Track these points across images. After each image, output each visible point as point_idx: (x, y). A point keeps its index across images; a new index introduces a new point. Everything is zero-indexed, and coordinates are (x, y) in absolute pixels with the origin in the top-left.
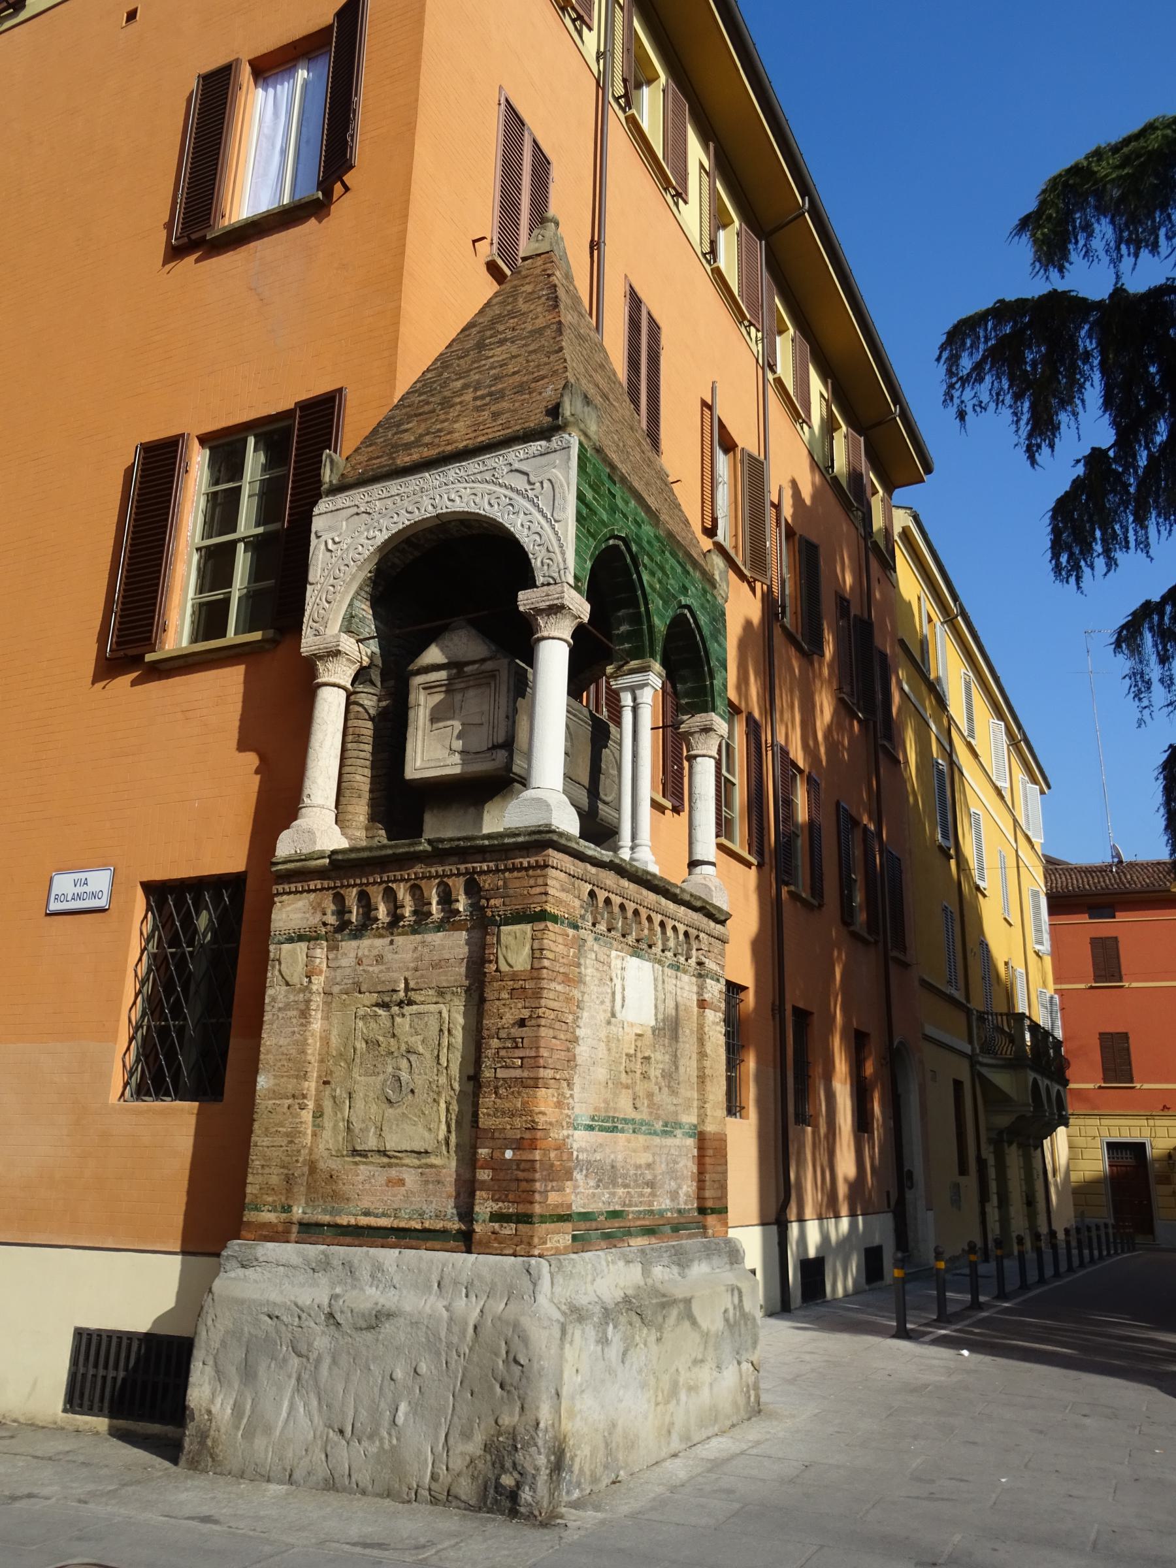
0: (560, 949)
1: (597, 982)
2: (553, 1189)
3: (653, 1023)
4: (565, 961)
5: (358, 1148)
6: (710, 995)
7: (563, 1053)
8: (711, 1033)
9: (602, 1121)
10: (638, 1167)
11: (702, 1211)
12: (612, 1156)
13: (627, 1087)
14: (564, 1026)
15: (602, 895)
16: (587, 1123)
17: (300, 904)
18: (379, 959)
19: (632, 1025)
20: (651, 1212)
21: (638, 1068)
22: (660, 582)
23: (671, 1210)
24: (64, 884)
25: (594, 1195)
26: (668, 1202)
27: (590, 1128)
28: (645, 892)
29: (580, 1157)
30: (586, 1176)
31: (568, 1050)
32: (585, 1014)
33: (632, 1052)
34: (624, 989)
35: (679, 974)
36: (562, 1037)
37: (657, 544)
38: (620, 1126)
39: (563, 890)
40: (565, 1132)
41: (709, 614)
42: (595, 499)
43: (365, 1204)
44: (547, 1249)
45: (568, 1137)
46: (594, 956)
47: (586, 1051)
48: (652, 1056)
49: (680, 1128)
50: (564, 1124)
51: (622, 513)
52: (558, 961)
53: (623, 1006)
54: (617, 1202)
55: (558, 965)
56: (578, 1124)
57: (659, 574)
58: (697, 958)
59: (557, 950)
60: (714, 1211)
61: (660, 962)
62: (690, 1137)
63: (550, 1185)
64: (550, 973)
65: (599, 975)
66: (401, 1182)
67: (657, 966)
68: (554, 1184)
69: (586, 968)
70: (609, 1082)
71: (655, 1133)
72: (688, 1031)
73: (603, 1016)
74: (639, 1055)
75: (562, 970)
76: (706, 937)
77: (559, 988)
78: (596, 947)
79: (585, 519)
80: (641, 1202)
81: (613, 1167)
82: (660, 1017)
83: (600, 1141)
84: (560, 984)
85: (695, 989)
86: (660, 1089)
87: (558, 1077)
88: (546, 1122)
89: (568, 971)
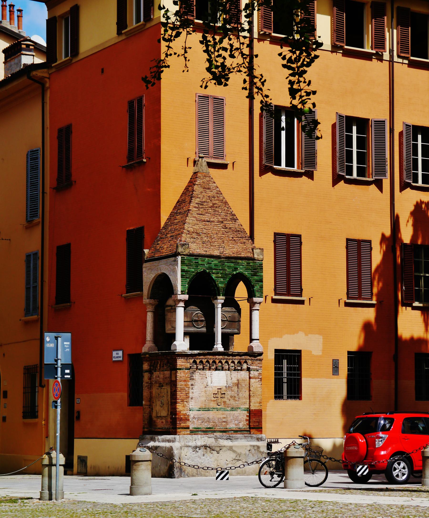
1: (200, 379)
4: (184, 377)
5: (158, 416)
6: (253, 375)
8: (253, 385)
11: (250, 428)
12: (208, 416)
14: (185, 391)
15: (198, 361)
17: (146, 364)
18: (159, 377)
19: (216, 387)
20: (227, 428)
21: (219, 396)
22: (221, 274)
24: (114, 354)
26: (234, 426)
27: (199, 410)
29: (195, 416)
31: (187, 395)
33: (216, 392)
36: (184, 393)
37: (220, 264)
38: (211, 410)
40: (186, 412)
41: (251, 270)
42: (188, 268)
43: (159, 427)
46: (199, 374)
48: (226, 393)
49: (240, 409)
50: (186, 410)
51: (202, 265)
57: (222, 271)
60: (253, 428)
61: (229, 370)
63: (181, 422)
65: (201, 377)
66: (163, 422)
69: (195, 376)
71: (227, 411)
72: (244, 385)
74: (219, 393)
77: (182, 383)
78: (199, 371)
79: (184, 275)
85: (248, 374)
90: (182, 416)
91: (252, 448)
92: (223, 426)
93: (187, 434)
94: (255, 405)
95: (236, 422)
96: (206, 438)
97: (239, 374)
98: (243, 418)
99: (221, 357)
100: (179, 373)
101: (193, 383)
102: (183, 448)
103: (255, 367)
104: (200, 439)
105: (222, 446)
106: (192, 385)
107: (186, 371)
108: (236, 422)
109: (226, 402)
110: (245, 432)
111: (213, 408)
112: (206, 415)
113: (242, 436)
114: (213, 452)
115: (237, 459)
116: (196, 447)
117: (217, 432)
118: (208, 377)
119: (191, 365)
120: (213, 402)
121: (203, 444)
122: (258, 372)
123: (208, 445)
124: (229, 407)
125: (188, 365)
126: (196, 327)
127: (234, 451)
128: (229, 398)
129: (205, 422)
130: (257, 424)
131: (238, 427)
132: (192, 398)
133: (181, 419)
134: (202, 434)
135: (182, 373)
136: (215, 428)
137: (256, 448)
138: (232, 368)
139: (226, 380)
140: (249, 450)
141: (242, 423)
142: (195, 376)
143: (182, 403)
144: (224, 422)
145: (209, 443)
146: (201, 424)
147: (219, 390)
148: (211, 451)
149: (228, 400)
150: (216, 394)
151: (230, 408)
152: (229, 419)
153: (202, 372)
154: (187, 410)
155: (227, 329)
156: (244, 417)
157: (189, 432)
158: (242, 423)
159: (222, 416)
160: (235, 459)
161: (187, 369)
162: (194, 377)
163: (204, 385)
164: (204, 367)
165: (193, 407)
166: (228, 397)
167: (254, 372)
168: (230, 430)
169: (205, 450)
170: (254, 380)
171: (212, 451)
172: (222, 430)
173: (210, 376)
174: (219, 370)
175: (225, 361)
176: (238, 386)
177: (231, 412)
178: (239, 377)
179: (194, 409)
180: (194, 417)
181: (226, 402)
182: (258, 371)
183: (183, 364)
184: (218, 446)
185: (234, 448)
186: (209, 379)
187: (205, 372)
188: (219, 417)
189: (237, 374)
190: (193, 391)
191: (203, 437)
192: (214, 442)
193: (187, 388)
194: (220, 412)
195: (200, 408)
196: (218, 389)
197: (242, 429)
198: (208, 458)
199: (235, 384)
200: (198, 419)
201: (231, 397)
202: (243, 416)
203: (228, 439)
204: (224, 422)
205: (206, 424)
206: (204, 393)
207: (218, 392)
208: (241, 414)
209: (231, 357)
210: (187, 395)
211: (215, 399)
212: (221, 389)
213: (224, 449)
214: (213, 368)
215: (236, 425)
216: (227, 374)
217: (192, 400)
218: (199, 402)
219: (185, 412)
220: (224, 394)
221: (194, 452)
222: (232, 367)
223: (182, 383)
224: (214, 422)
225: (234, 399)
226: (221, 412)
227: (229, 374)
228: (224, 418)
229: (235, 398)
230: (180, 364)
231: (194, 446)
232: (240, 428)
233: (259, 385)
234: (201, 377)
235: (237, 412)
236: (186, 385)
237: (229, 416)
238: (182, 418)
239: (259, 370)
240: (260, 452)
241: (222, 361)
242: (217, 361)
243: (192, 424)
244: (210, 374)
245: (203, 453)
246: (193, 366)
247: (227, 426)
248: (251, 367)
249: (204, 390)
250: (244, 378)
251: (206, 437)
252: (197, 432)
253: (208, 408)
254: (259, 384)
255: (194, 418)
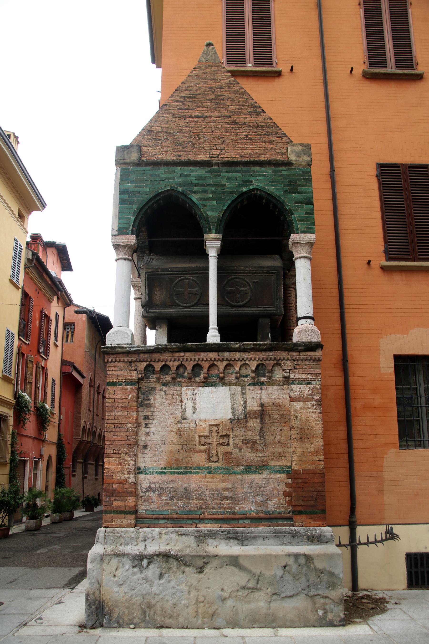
0: (119, 396)
1: (166, 405)
2: (115, 500)
3: (230, 416)
4: (124, 401)
7: (123, 442)
8: (298, 415)
9: (174, 469)
10: (213, 490)
12: (186, 485)
13: (201, 451)
14: (126, 430)
16: (159, 471)
19: (205, 421)
20: (234, 513)
21: (215, 441)
23: (257, 513)
25: (168, 504)
26: (253, 507)
28: (203, 354)
29: (153, 486)
30: (159, 495)
31: (128, 439)
32: (155, 422)
33: (206, 433)
34: (195, 404)
35: (264, 387)
39: (121, 370)
40: (127, 476)
44: (112, 525)
45: (129, 478)
46: (163, 393)
47: (156, 438)
48: (231, 434)
49: (268, 469)
50: (125, 472)
52: (118, 402)
53: (194, 413)
54: (192, 507)
55: (116, 403)
56: (150, 472)
58: (283, 375)
59: (116, 397)
62: (283, 472)
63: (113, 499)
64: (110, 408)
65: (168, 401)
67: (234, 387)
68: (117, 498)
69: (155, 399)
70: (181, 451)
71: (235, 473)
73: (172, 420)
75: (120, 405)
76: (288, 363)
78: (165, 388)
80: (220, 507)
81: (186, 490)
82: (239, 411)
83: (173, 478)
84: (118, 412)
86: (240, 450)
87: (120, 452)
88: (109, 472)
89: (127, 405)
90: (115, 486)
91: (291, 561)
92: (225, 508)
93: (129, 526)
94: (304, 459)
95: (258, 498)
96: (174, 536)
97: (264, 391)
98: (276, 489)
99: (212, 355)
100: (112, 392)
101: (149, 414)
102: (107, 559)
103: (304, 376)
104: (157, 537)
105: (209, 556)
106: (146, 418)
107: (129, 387)
108: (259, 498)
109: (231, 453)
110: (280, 522)
111: (200, 468)
112: (180, 483)
113: (269, 532)
114: (187, 569)
115: (250, 585)
116: (141, 557)
117: (206, 521)
118: (185, 401)
119: (140, 376)
120: (197, 454)
121: (163, 548)
122: (311, 386)
123: (173, 553)
124: (239, 465)
125: (134, 375)
126: (180, 306)
127: (241, 568)
128: (240, 444)
129: (178, 499)
130: (312, 503)
131: (263, 509)
132: (145, 447)
133: (114, 493)
134: (168, 526)
135: (119, 392)
136: (204, 513)
137: (302, 560)
138: (246, 379)
139: (229, 406)
140: (285, 567)
141: (275, 500)
142: (155, 399)
143: (118, 456)
144: (227, 498)
145: (177, 548)
146: (168, 503)
147: (215, 429)
148: (180, 567)
149: (237, 450)
150: (207, 436)
151: (241, 468)
152: (240, 492)
153: (171, 390)
154: (129, 473)
155: (252, 306)
156: (279, 487)
157: (133, 522)
158: (275, 500)
159: (221, 486)
160: (244, 588)
161: (129, 383)
162: (152, 401)
163: (175, 418)
164: (174, 379)
165: (149, 465)
166: (237, 442)
167: (300, 386)
168: (241, 516)
169: (164, 565)
170: (301, 403)
171: (183, 568)
172: (220, 517)
173: (190, 397)
174: (213, 385)
175: (225, 363)
176: (261, 419)
177: (246, 477)
178: (265, 399)
179: (151, 470)
180: (150, 487)
181: (231, 453)
182: (310, 383)
183: (122, 372)
184: (199, 556)
185: (242, 561)
186: (189, 405)
187: (178, 389)
188: (214, 488)
189: (259, 392)
190: (147, 430)
191: (166, 534)
192: (194, 545)
193: (130, 425)
194: (217, 476)
195: (165, 468)
196: (210, 425)
197: (272, 516)
198: (173, 583)
199: (255, 412)
200: (161, 491)
201: (245, 442)
202: (276, 485)
203: (230, 538)
204: (227, 498)
205: (180, 504)
206: (175, 434)
207: (211, 432)
208: (270, 480)
209: (237, 355)
210: (128, 439)
211: (204, 448)
212: (219, 425)
213: (215, 563)
214: (197, 379)
215: (257, 504)
216: (233, 392)
217: (146, 451)
218: (163, 454)
219: (123, 477)
220: (227, 436)
221: (136, 570)
222: (246, 376)
223: (117, 414)
224: (202, 499)
225: (251, 448)
226: (219, 477)
227: (240, 393)
228: (228, 489)
229: (256, 446)
230: (114, 373)
231: (137, 555)
232: (268, 513)
233: (314, 415)
234: (168, 401)
235: (261, 476)
236: (126, 418)
237: (239, 486)
238: (115, 490)
239: (314, 383)
240: (316, 569)
241: (219, 364)
242: (206, 366)
243: (145, 504)
244: (190, 392)
245: (158, 571)
246: (148, 378)
247: (234, 508)
248: (292, 376)
249: (175, 428)
250: (277, 401)
251: (173, 533)
252: (156, 522)
253: (186, 468)
254: (315, 413)
255: (150, 489)
